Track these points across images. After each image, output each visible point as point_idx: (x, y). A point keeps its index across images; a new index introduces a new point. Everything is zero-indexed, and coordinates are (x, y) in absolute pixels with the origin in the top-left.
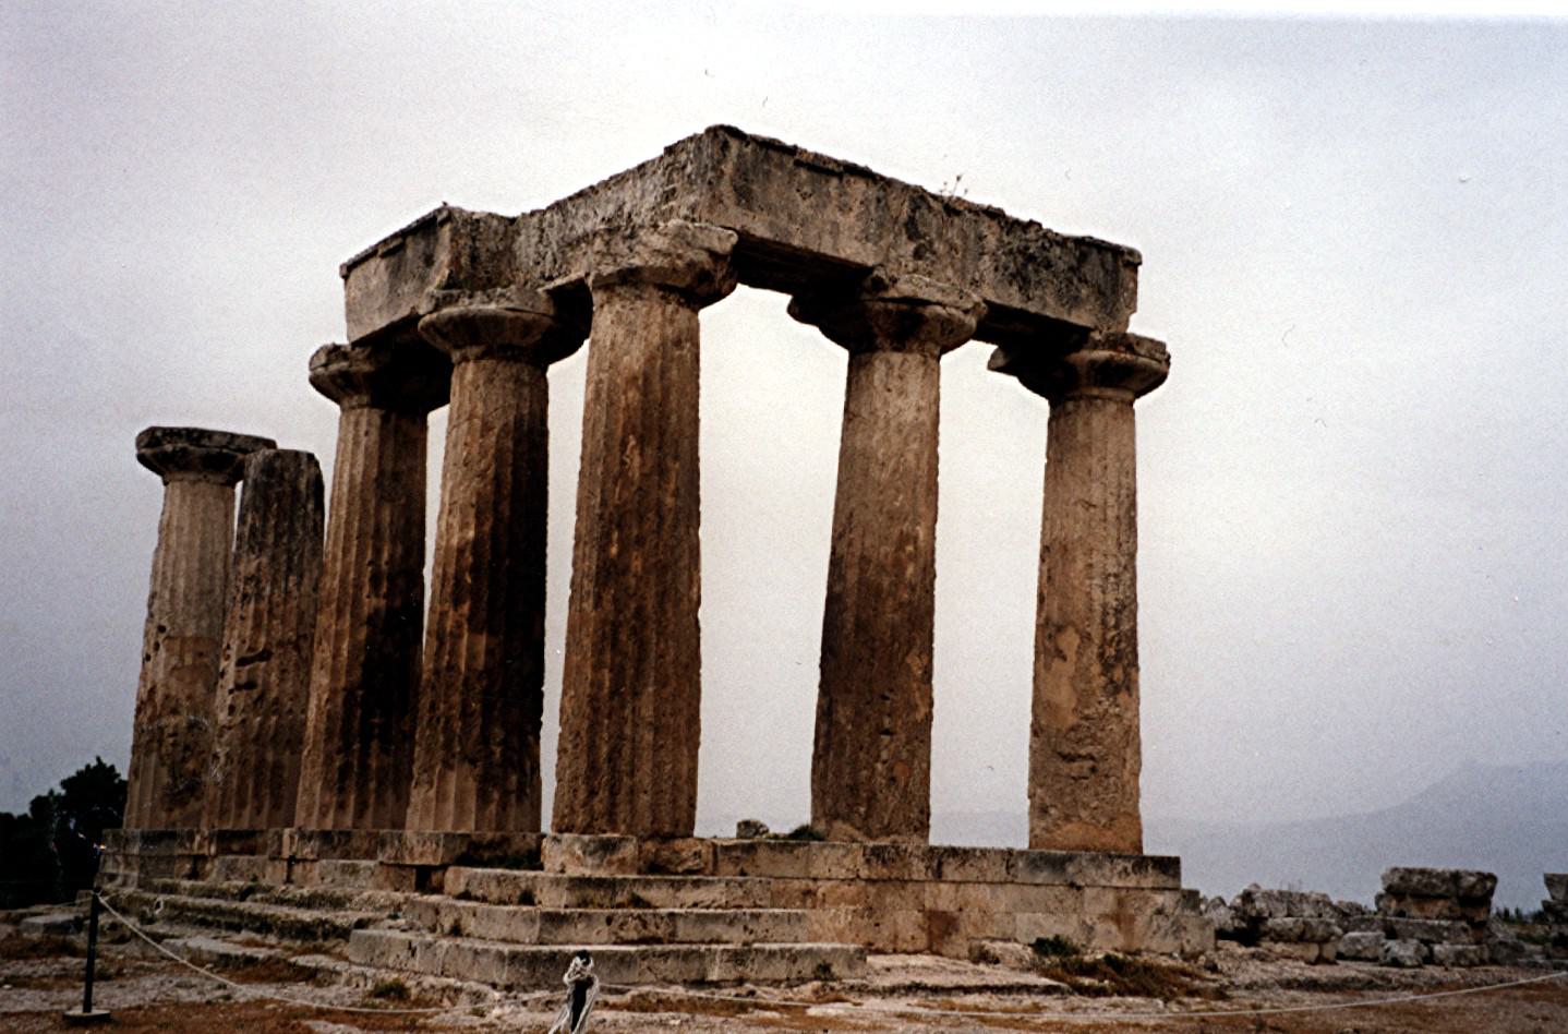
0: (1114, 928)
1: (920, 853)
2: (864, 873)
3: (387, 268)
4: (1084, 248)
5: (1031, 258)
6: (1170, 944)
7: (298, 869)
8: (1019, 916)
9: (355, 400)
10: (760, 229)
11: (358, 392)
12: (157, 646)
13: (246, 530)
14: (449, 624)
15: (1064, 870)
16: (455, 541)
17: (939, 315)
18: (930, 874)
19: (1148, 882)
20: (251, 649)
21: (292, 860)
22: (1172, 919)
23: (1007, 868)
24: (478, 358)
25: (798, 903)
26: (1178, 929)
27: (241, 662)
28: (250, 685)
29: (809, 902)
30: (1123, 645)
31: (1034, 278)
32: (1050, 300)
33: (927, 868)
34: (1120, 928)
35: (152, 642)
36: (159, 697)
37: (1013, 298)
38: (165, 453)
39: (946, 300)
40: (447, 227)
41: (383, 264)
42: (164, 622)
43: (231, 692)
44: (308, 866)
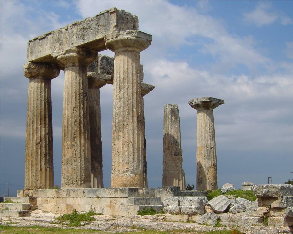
0: (109, 209)
1: (65, 191)
2: (55, 196)
4: (99, 17)
5: (86, 28)
6: (125, 214)
8: (86, 206)
10: (34, 58)
15: (96, 193)
17: (59, 58)
18: (67, 196)
19: (118, 196)
22: (126, 206)
23: (83, 193)
25: (45, 203)
26: (127, 209)
29: (47, 203)
30: (117, 126)
31: (86, 34)
32: (91, 37)
33: (67, 194)
34: (111, 208)
37: (82, 42)
39: (59, 54)
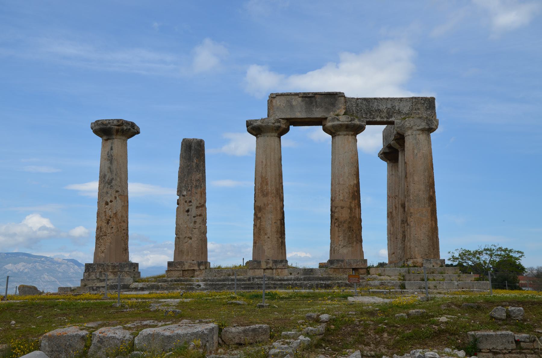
3: (302, 101)
7: (267, 271)
9: (273, 134)
11: (276, 132)
12: (116, 198)
13: (194, 164)
14: (353, 205)
16: (352, 183)
20: (200, 204)
21: (264, 269)
24: (352, 135)
27: (197, 207)
28: (200, 215)
35: (114, 196)
36: (119, 215)
38: (123, 129)
40: (343, 98)
41: (300, 99)
42: (119, 190)
43: (194, 217)
44: (279, 270)
